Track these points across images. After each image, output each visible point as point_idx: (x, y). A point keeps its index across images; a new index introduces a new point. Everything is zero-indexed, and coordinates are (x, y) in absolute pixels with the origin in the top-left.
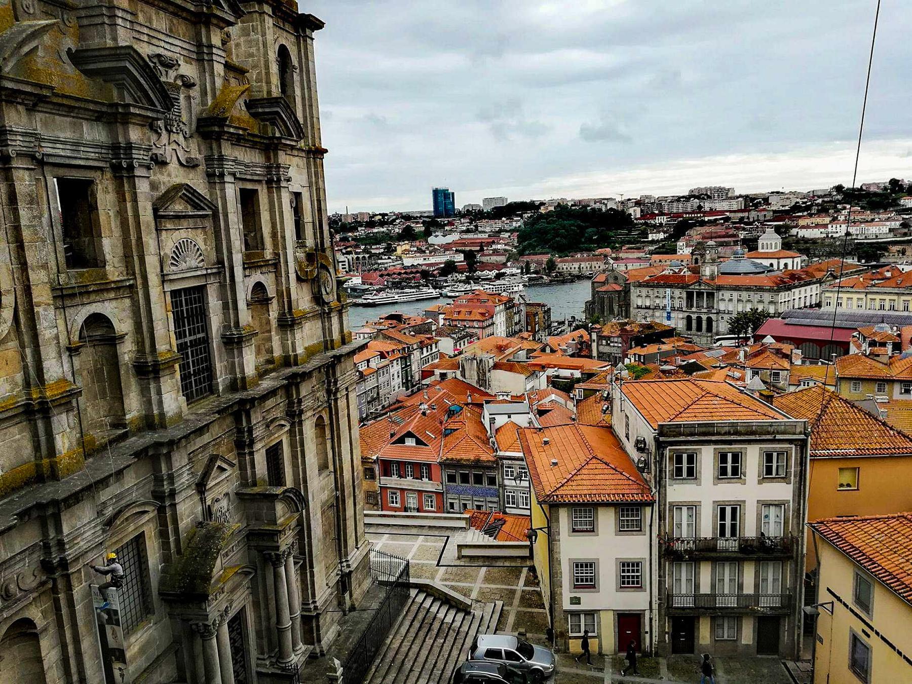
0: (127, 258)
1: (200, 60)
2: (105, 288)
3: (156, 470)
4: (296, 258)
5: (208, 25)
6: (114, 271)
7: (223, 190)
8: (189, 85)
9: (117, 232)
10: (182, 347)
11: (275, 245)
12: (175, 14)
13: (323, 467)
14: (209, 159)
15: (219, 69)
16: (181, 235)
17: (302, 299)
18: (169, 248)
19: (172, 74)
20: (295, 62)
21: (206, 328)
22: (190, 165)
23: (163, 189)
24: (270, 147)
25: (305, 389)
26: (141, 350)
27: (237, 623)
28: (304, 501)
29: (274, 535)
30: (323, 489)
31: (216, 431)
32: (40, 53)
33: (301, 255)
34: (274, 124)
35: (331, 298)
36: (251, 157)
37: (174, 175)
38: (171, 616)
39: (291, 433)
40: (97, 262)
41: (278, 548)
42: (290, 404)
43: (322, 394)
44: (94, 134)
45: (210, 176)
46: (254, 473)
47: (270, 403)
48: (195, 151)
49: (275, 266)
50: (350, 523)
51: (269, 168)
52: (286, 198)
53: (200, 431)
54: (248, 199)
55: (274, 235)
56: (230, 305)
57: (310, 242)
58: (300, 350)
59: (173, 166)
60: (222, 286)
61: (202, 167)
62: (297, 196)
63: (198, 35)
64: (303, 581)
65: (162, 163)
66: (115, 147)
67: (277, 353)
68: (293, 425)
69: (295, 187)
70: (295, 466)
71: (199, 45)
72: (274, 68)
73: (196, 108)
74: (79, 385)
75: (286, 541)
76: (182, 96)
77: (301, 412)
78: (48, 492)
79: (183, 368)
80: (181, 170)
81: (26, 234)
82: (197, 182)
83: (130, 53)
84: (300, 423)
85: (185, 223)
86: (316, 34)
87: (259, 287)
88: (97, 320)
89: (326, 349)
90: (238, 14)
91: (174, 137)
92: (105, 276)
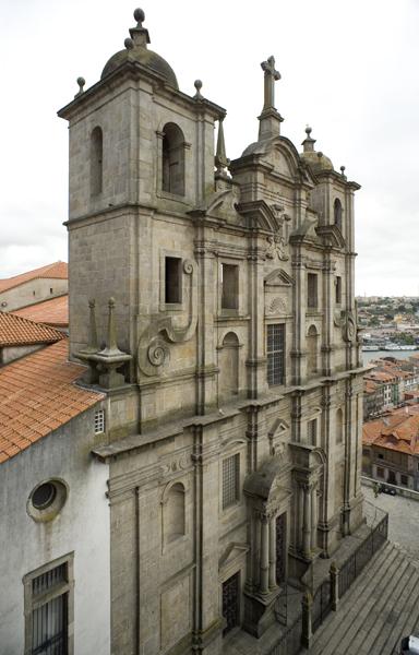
0: (249, 305)
1: (294, 207)
2: (237, 319)
3: (250, 420)
4: (335, 314)
5: (299, 189)
6: (242, 309)
7: (299, 273)
8: (287, 219)
9: (246, 292)
10: (269, 356)
11: (324, 305)
12: (285, 185)
13: (339, 440)
14: (294, 256)
15: (303, 210)
16: (275, 296)
17: (336, 337)
18: (269, 304)
19: (280, 214)
20: (343, 206)
21: (283, 347)
22: (284, 259)
23: (270, 271)
24: (326, 250)
25: (333, 391)
26: (249, 356)
27: (281, 520)
28: (326, 456)
29: (308, 473)
30: (337, 454)
31: (282, 405)
32: (224, 205)
33: (338, 312)
34: (329, 239)
35: (352, 338)
36: (317, 257)
37: (276, 265)
38: (247, 505)
39: (322, 415)
40: (235, 307)
41: (308, 482)
42: (323, 399)
43: (342, 395)
44: (242, 243)
45: (293, 265)
46: (299, 435)
47: (312, 395)
48: (287, 251)
49: (324, 318)
50: (352, 479)
51: (324, 262)
52: (332, 280)
53: (274, 403)
54: (312, 278)
55: (324, 299)
56: (296, 336)
57: (343, 304)
58: (332, 367)
59: (276, 260)
60: (294, 325)
61: (290, 262)
62: (338, 278)
63: (295, 196)
64: (321, 507)
65: (269, 257)
66: (250, 249)
67: (319, 367)
68: (324, 410)
69: (338, 274)
70: (322, 436)
71: (295, 199)
72: (332, 210)
73: (290, 231)
74: (220, 367)
75: (313, 479)
76: (284, 225)
77: (329, 404)
78: (198, 420)
79: (269, 367)
80: (280, 262)
81: (206, 289)
82: (287, 269)
83: (262, 203)
84: (328, 411)
85: (278, 289)
86: (356, 192)
87: (313, 327)
88: (231, 335)
89: (347, 369)
90: (316, 183)
91: (278, 245)
92: (237, 313)
